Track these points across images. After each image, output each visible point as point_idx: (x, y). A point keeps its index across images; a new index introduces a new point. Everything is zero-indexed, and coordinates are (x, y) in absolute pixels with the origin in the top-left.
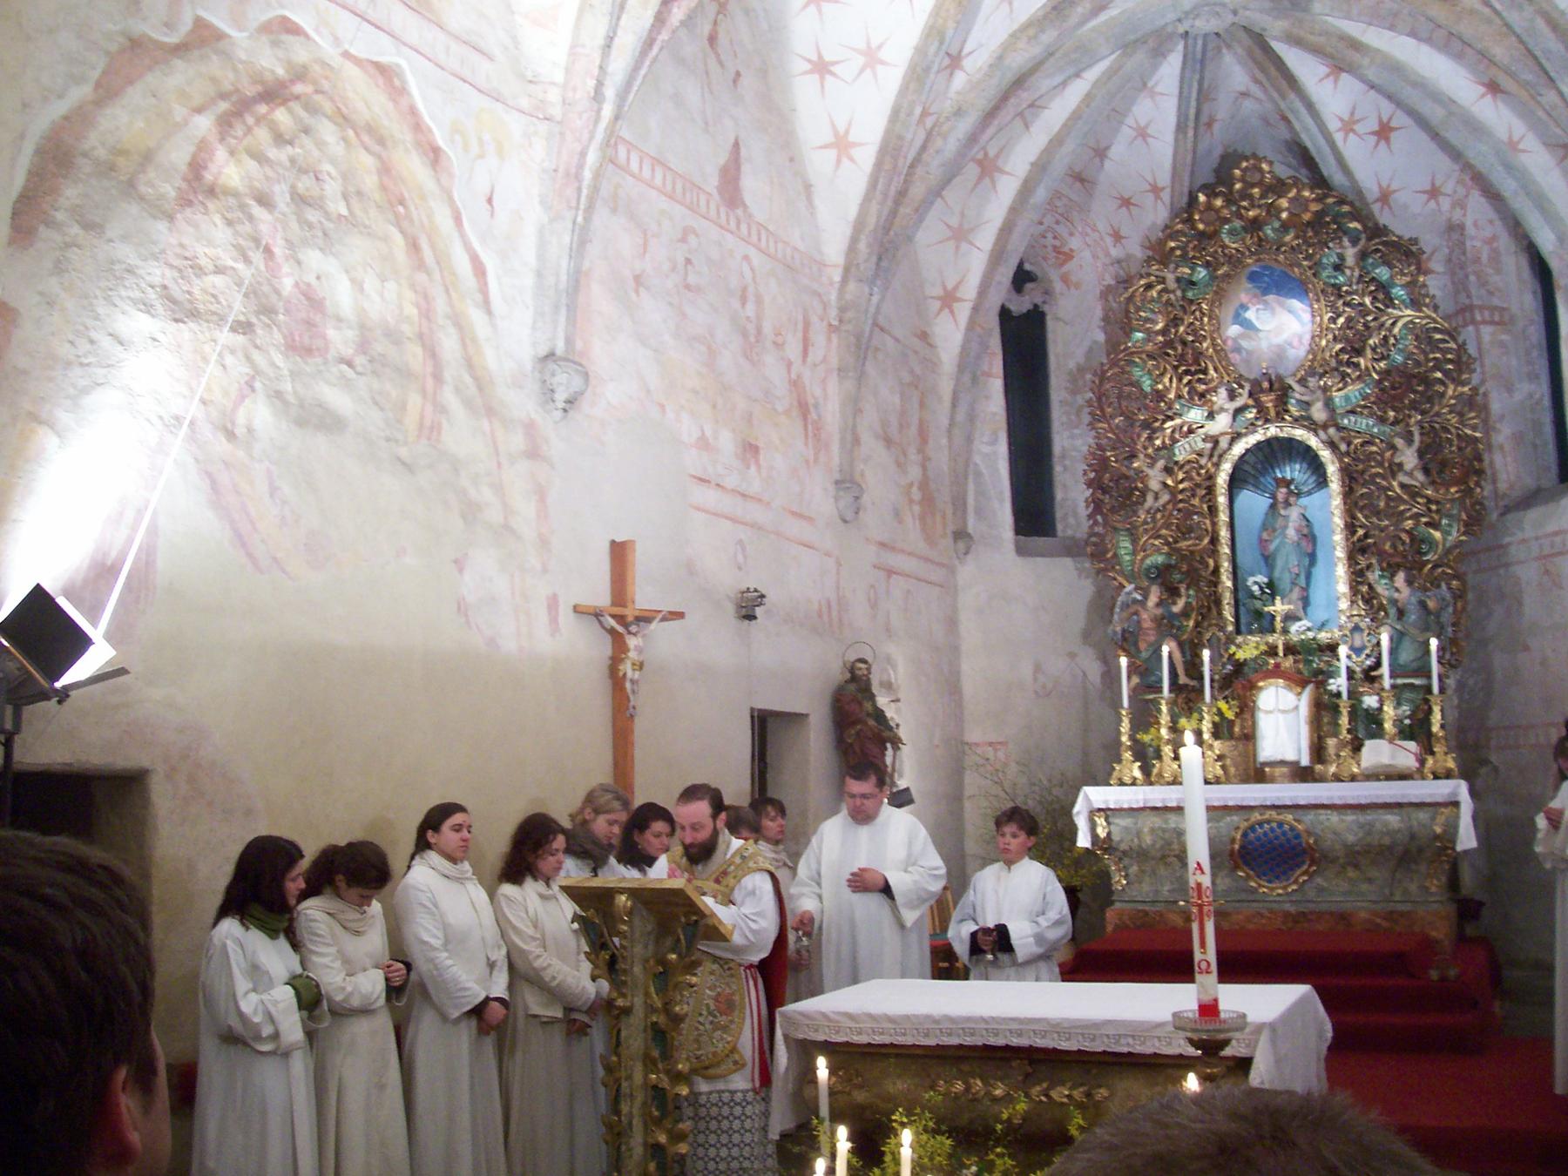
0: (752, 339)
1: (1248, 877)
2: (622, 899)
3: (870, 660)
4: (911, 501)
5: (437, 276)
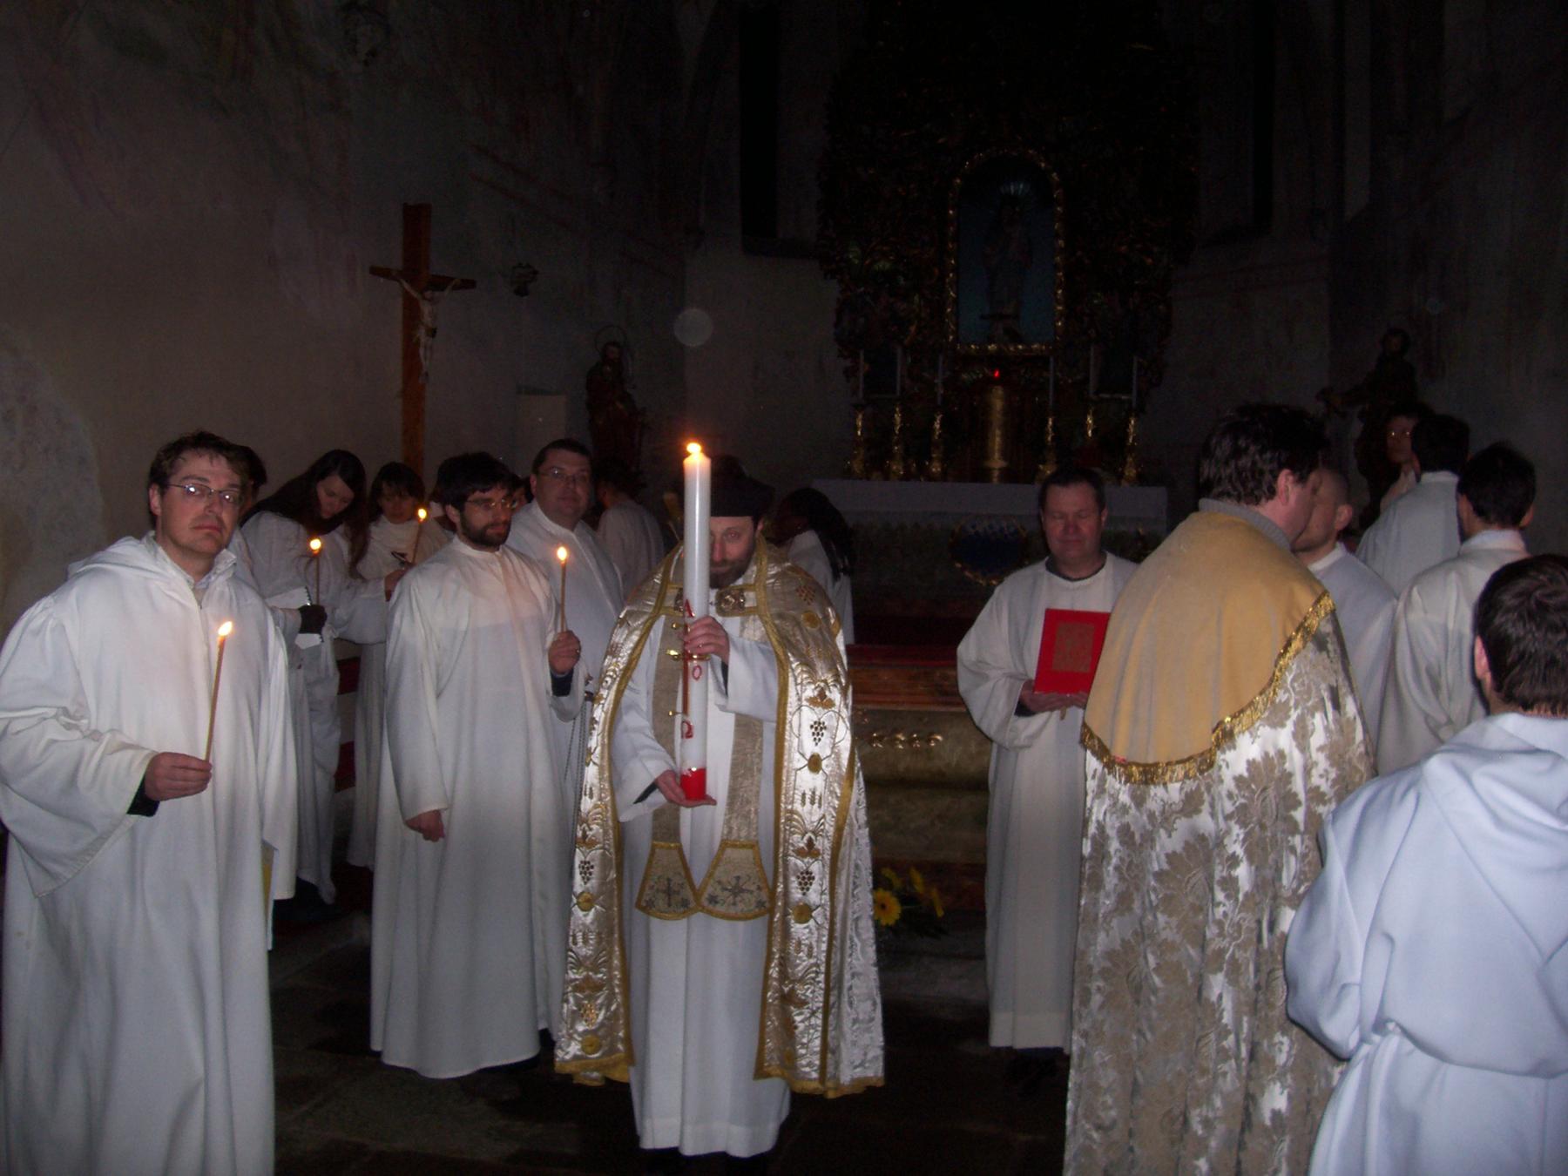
1: (963, 569)
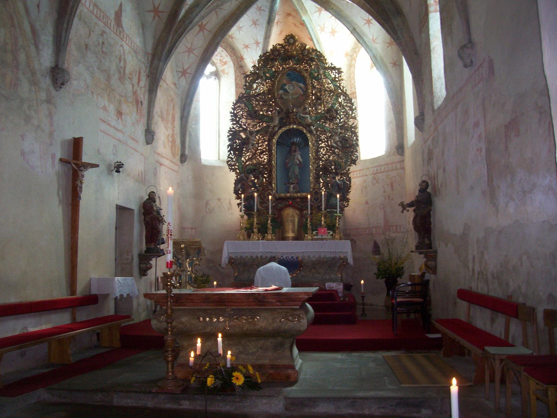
3: (155, 191)
4: (169, 141)
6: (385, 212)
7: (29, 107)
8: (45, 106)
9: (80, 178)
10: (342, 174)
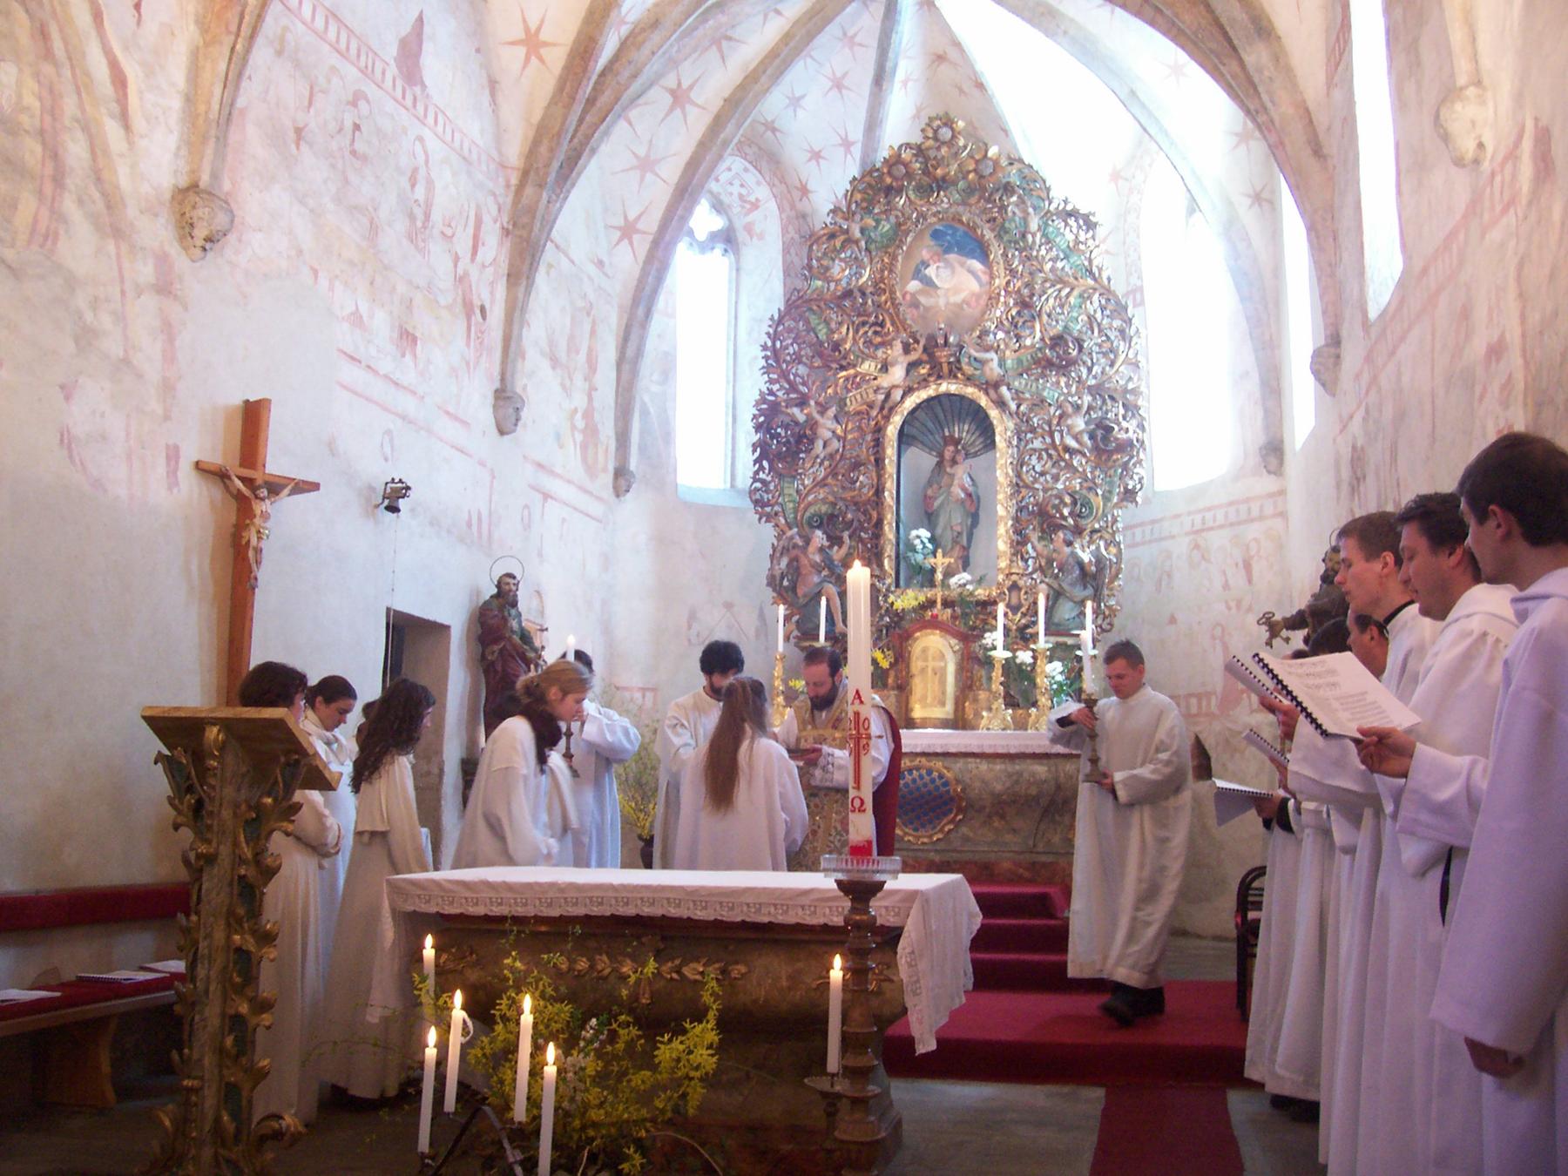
0: (419, 224)
2: (213, 733)
4: (573, 427)
5: (68, 73)
6: (1225, 647)
7: (95, 303)
8: (149, 301)
9: (257, 521)
10: (1094, 531)
